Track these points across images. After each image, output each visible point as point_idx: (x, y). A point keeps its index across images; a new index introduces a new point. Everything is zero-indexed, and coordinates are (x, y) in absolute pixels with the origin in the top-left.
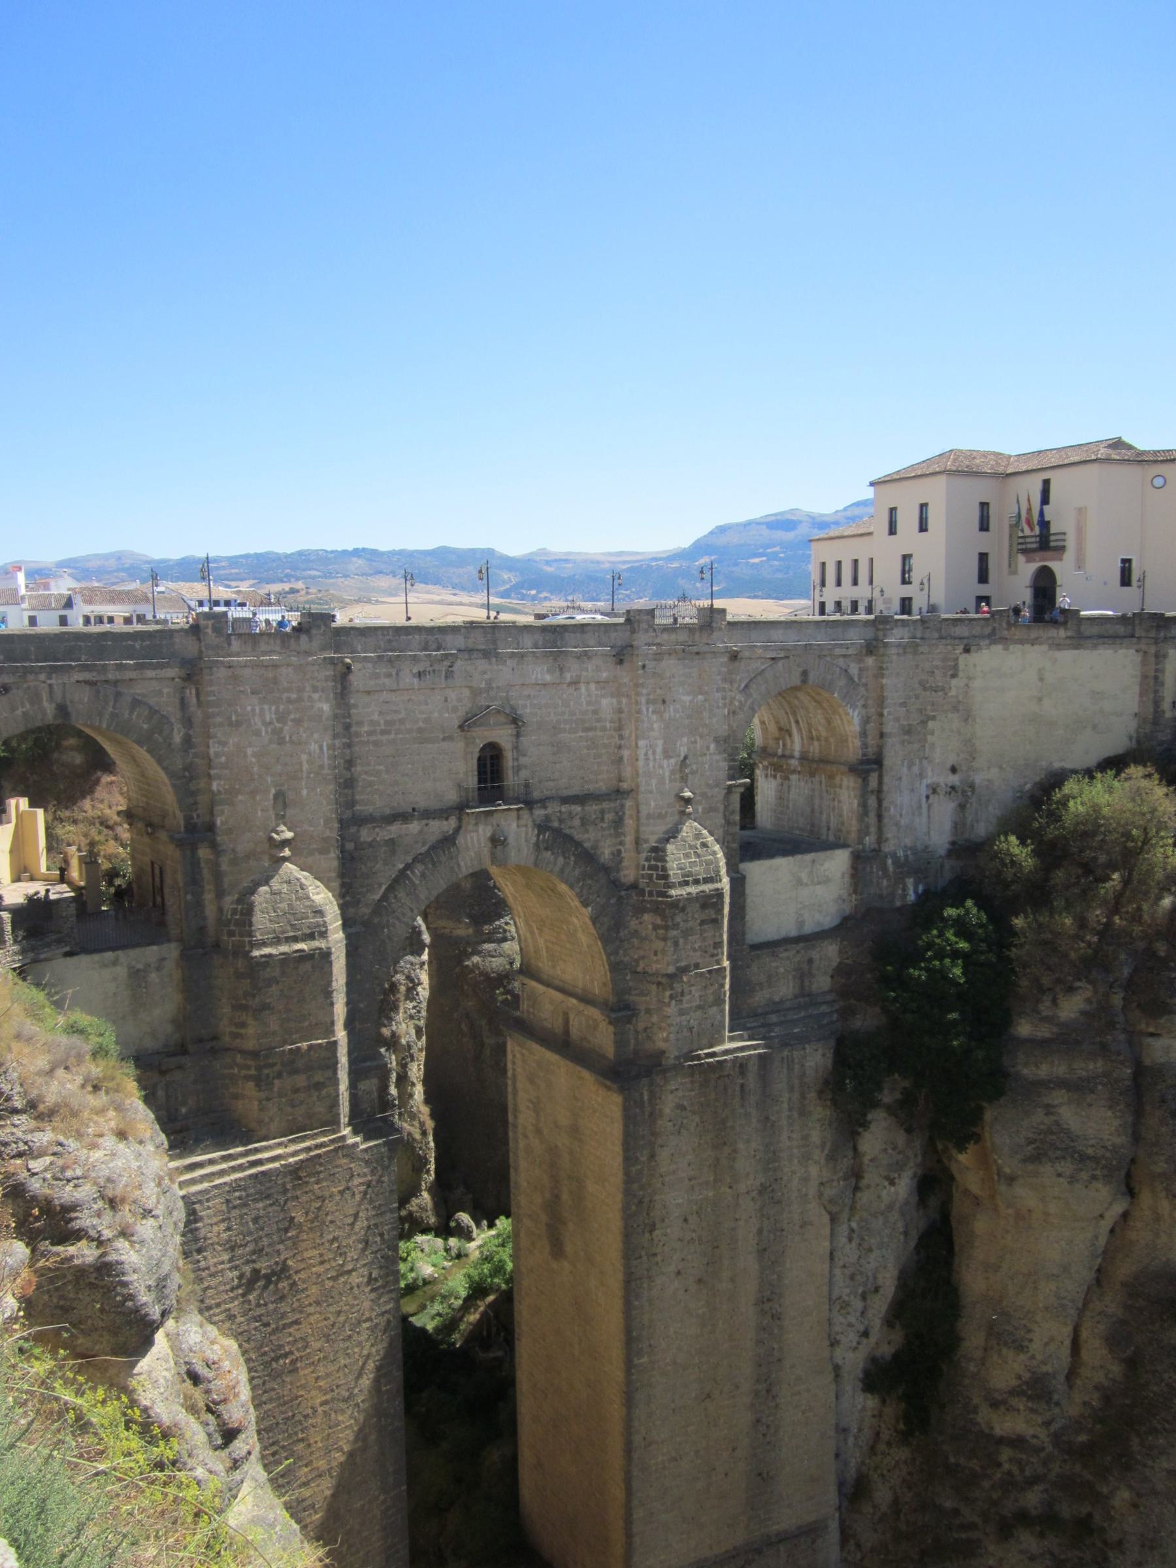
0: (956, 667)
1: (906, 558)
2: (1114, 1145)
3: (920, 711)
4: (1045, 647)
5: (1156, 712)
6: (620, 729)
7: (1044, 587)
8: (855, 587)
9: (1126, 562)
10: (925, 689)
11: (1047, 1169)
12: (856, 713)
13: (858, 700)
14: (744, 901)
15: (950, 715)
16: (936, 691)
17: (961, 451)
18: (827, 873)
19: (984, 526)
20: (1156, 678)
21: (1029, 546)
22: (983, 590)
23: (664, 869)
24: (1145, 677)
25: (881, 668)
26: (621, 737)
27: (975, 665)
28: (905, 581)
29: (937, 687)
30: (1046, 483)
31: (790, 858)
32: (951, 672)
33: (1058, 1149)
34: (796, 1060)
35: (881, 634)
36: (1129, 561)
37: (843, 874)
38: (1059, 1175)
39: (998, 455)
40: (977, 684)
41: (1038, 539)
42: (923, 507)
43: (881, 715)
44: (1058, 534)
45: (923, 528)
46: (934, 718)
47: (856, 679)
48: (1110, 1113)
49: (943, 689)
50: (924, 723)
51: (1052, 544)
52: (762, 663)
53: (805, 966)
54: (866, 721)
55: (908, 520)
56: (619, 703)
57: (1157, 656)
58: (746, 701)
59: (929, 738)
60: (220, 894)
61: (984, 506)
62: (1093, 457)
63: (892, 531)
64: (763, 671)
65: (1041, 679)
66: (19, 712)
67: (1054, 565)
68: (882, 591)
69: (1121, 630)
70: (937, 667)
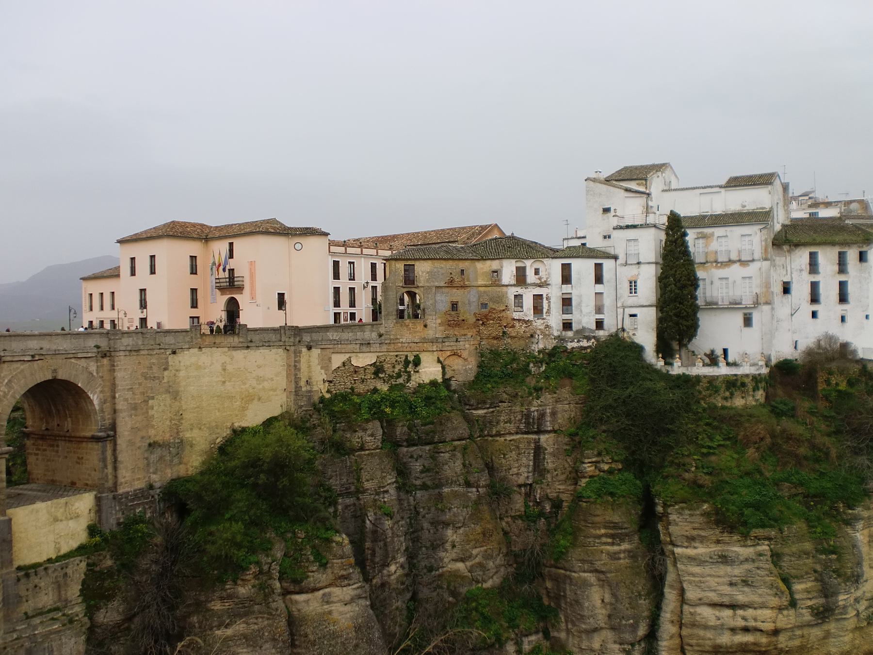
0: (167, 363)
1: (143, 291)
3: (143, 393)
5: (296, 387)
7: (233, 310)
8: (102, 312)
9: (281, 296)
10: (146, 379)
12: (96, 396)
13: (97, 389)
14: (11, 537)
15: (164, 396)
16: (153, 380)
17: (178, 222)
18: (77, 511)
19: (194, 271)
20: (295, 366)
21: (222, 284)
22: (194, 312)
25: (114, 366)
27: (180, 362)
28: (143, 305)
29: (154, 377)
30: (231, 244)
31: (49, 503)
32: (164, 367)
34: (55, 649)
35: (112, 342)
36: (283, 294)
37: (90, 510)
39: (202, 225)
40: (182, 374)
41: (228, 280)
43: (114, 397)
44: (239, 277)
45: (153, 272)
46: (153, 398)
47: (95, 374)
49: (158, 378)
50: (146, 402)
51: (236, 283)
52: (22, 364)
53: (60, 579)
54: (103, 402)
55: (143, 266)
57: (295, 352)
58: (9, 392)
59: (150, 411)
62: (258, 230)
63: (133, 273)
64: (22, 371)
65: (224, 370)
67: (237, 297)
68: (125, 314)
69: (273, 337)
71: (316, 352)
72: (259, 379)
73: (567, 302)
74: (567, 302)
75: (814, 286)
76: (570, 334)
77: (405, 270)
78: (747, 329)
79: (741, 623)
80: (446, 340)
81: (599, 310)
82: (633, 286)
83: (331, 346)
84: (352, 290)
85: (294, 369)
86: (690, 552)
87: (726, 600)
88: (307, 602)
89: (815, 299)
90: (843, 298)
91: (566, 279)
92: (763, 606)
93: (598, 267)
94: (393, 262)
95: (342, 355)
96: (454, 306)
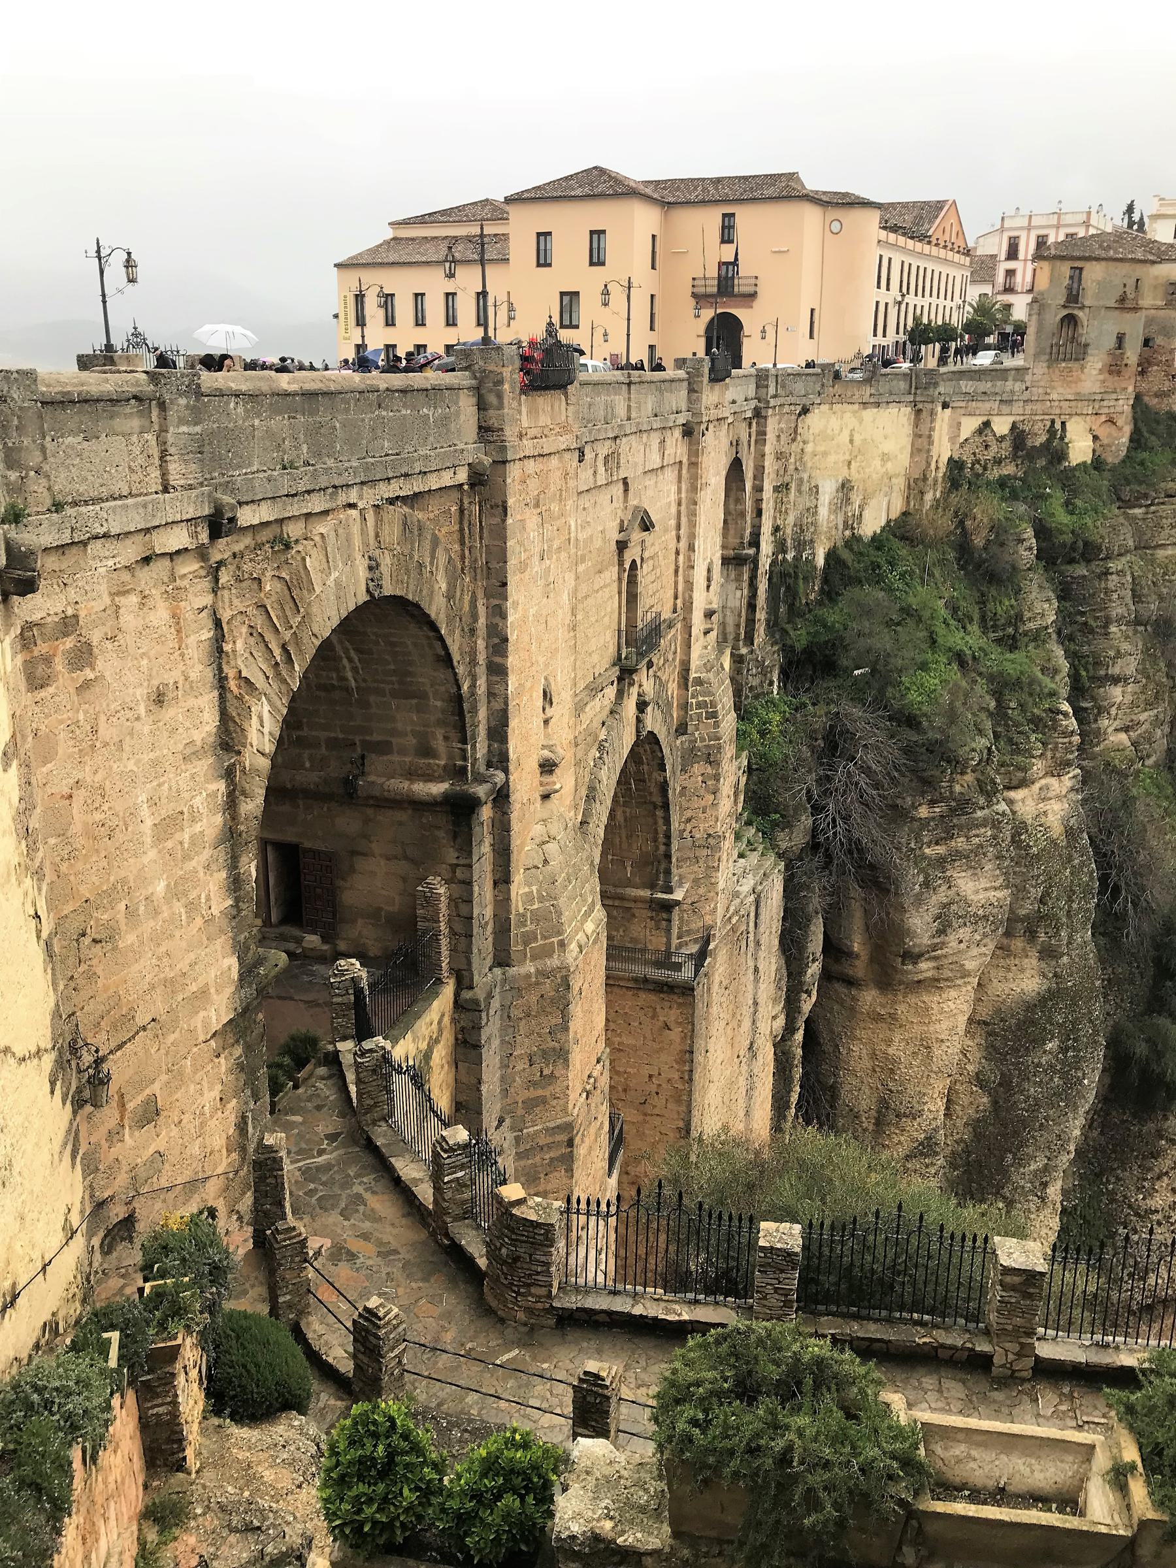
2: (998, 900)
4: (856, 406)
6: (678, 527)
11: (952, 939)
23: (713, 704)
24: (917, 436)
26: (678, 538)
33: (960, 917)
38: (961, 942)
40: (809, 448)
41: (716, 282)
42: (597, 235)
44: (746, 277)
45: (596, 260)
48: (998, 872)
51: (736, 289)
56: (679, 491)
60: (503, 880)
61: (654, 236)
63: (543, 261)
65: (851, 441)
66: (331, 581)
67: (738, 312)
70: (782, 430)
71: (948, 411)
72: (885, 458)
77: (1071, 278)
80: (1106, 396)
83: (963, 404)
84: (887, 304)
85: (921, 441)
88: (1023, 800)
94: (1058, 263)
95: (974, 418)
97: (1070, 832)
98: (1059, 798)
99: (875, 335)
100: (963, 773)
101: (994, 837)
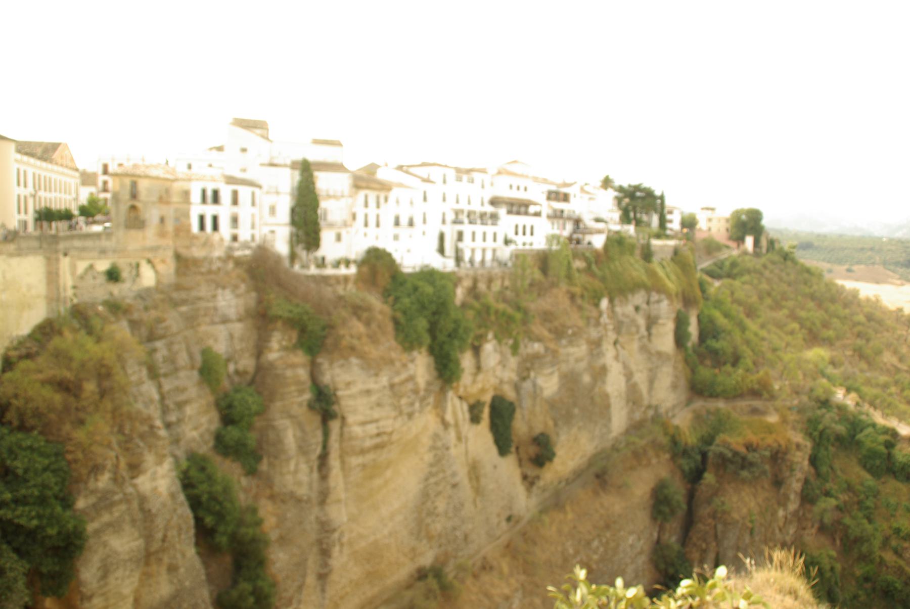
11: (111, 580)
73: (235, 220)
74: (235, 220)
75: (366, 216)
76: (236, 245)
78: (338, 244)
79: (375, 431)
81: (253, 227)
82: (273, 210)
85: (52, 277)
86: (348, 392)
87: (368, 419)
89: (366, 225)
90: (378, 225)
91: (235, 202)
92: (388, 418)
93: (253, 194)
96: (162, 220)
97: (173, 496)
98: (163, 477)
99: (19, 212)
100: (103, 474)
101: (129, 509)
